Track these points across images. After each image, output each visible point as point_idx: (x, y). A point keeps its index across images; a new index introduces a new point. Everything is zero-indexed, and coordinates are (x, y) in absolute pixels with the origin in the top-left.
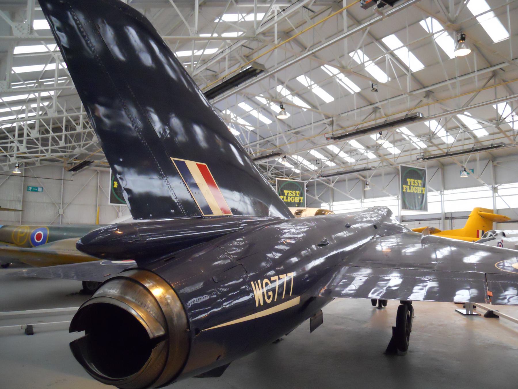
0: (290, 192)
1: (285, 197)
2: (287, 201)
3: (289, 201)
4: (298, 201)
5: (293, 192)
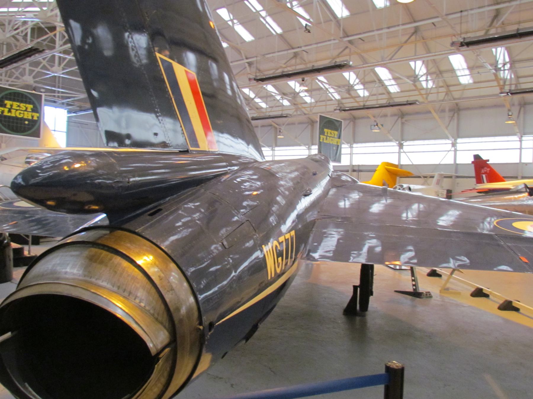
0: (15, 104)
1: (6, 110)
2: (9, 114)
3: (13, 115)
4: (30, 118)
5: (22, 105)
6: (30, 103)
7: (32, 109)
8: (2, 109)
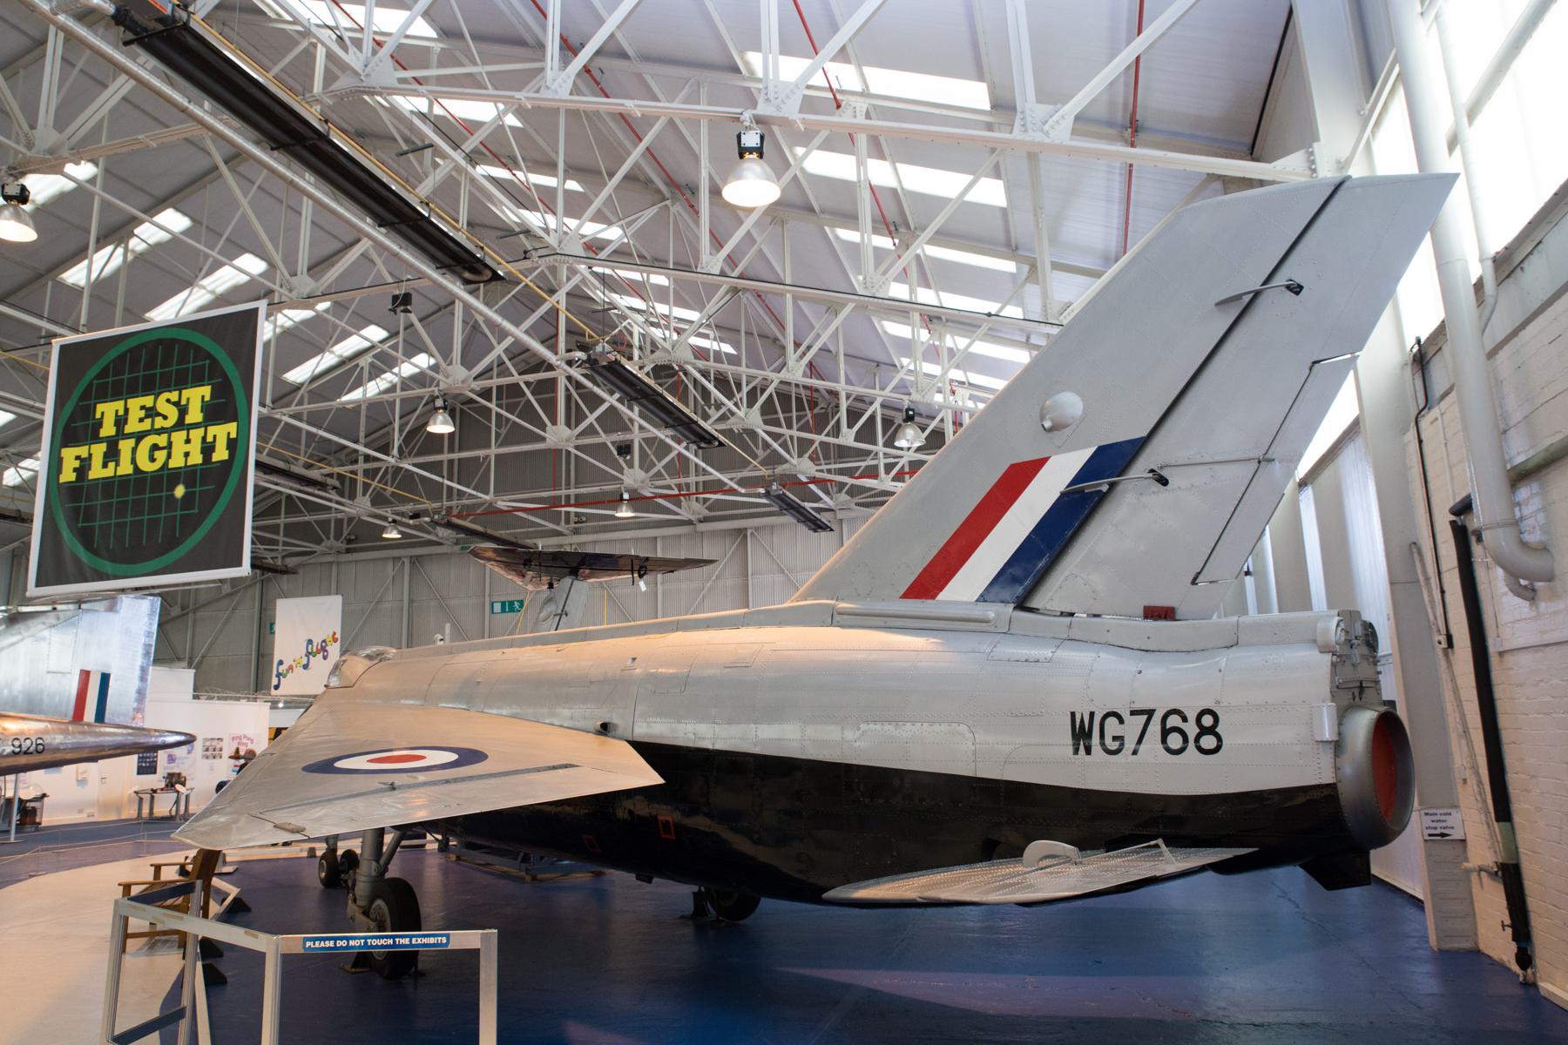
0: (135, 404)
1: (99, 450)
2: (109, 472)
3: (125, 468)
5: (164, 403)
6: (198, 381)
8: (83, 451)
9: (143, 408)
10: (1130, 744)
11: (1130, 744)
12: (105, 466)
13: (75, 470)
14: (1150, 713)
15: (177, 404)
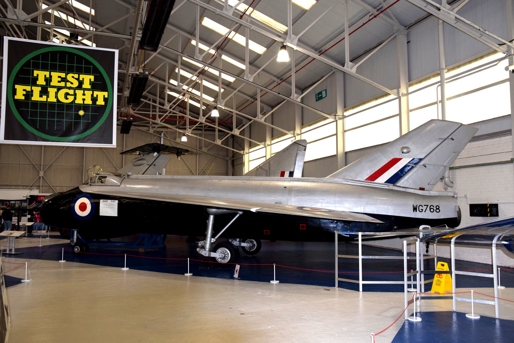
0: (56, 76)
1: (37, 90)
2: (44, 98)
3: (52, 99)
4: (89, 102)
5: (70, 77)
6: (87, 72)
7: (91, 83)
8: (28, 88)
9: (59, 77)
10: (424, 211)
11: (424, 211)
12: (41, 96)
13: (24, 95)
14: (428, 206)
15: (78, 79)
